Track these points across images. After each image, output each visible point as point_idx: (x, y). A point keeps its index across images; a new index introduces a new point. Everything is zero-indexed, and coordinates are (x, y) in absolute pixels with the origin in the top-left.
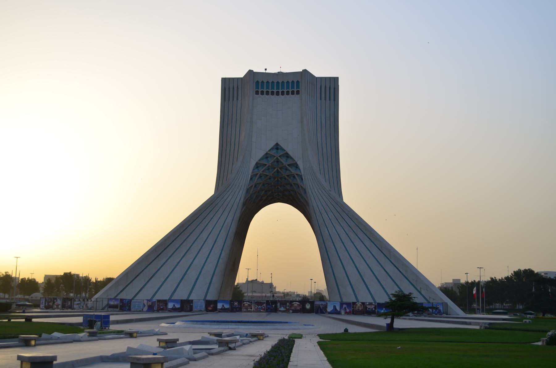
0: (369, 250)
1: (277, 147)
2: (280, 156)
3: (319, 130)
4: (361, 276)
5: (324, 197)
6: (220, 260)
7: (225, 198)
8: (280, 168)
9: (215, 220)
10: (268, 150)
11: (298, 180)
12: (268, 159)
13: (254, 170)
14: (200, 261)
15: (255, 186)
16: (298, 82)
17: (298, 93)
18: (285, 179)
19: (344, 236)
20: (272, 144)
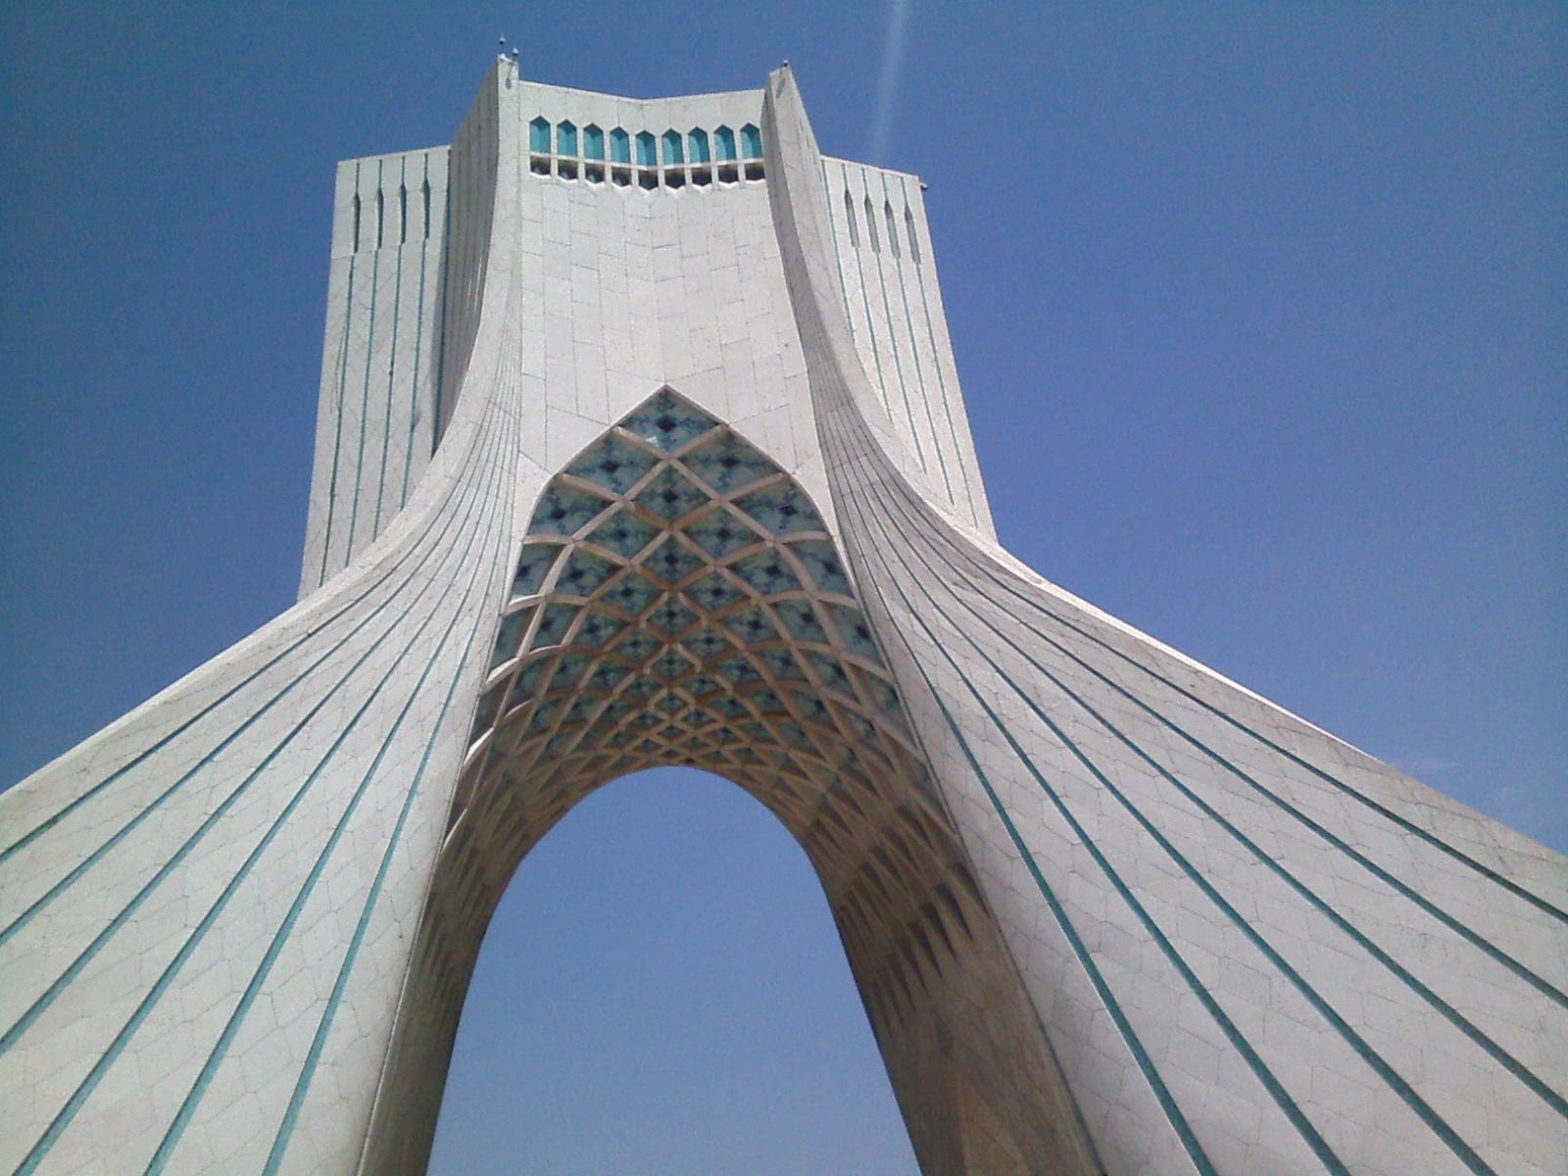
1: (666, 412)
2: (683, 460)
4: (1402, 1088)
5: (1004, 620)
6: (320, 1071)
7: (361, 643)
9: (285, 776)
10: (617, 419)
11: (805, 578)
12: (619, 473)
13: (536, 523)
15: (545, 625)
16: (750, 130)
17: (754, 173)
18: (718, 592)
20: (636, 396)
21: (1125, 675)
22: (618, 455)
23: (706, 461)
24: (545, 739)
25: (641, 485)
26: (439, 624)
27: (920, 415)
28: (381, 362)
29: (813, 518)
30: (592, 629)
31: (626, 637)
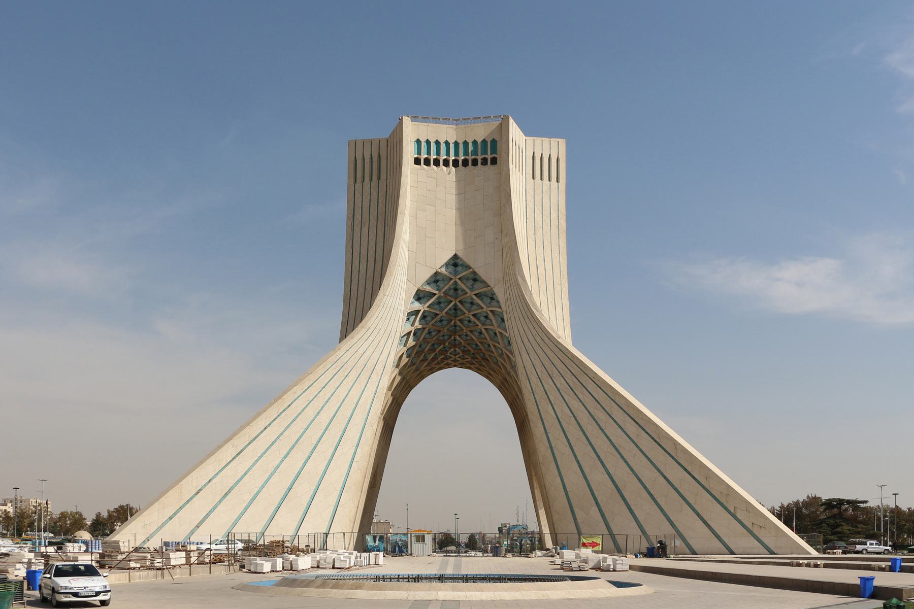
0: (633, 442)
1: (455, 262)
2: (460, 279)
3: (531, 232)
7: (361, 352)
8: (460, 302)
9: (343, 390)
14: (316, 466)
18: (469, 321)
19: (585, 420)
21: (576, 370)
22: (438, 277)
23: (468, 279)
24: (414, 367)
25: (447, 287)
26: (382, 344)
27: (548, 250)
28: (365, 230)
29: (498, 302)
30: (429, 333)
31: (441, 334)
